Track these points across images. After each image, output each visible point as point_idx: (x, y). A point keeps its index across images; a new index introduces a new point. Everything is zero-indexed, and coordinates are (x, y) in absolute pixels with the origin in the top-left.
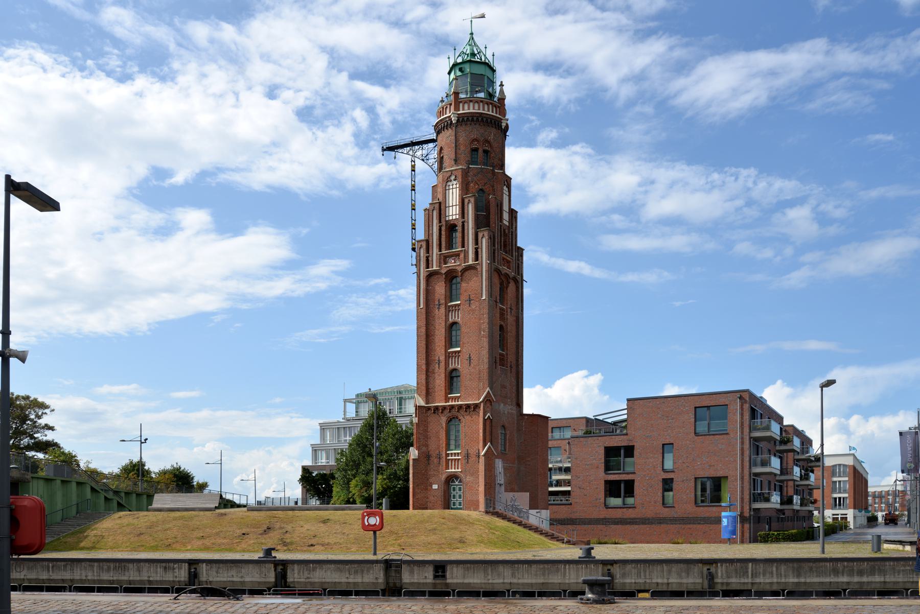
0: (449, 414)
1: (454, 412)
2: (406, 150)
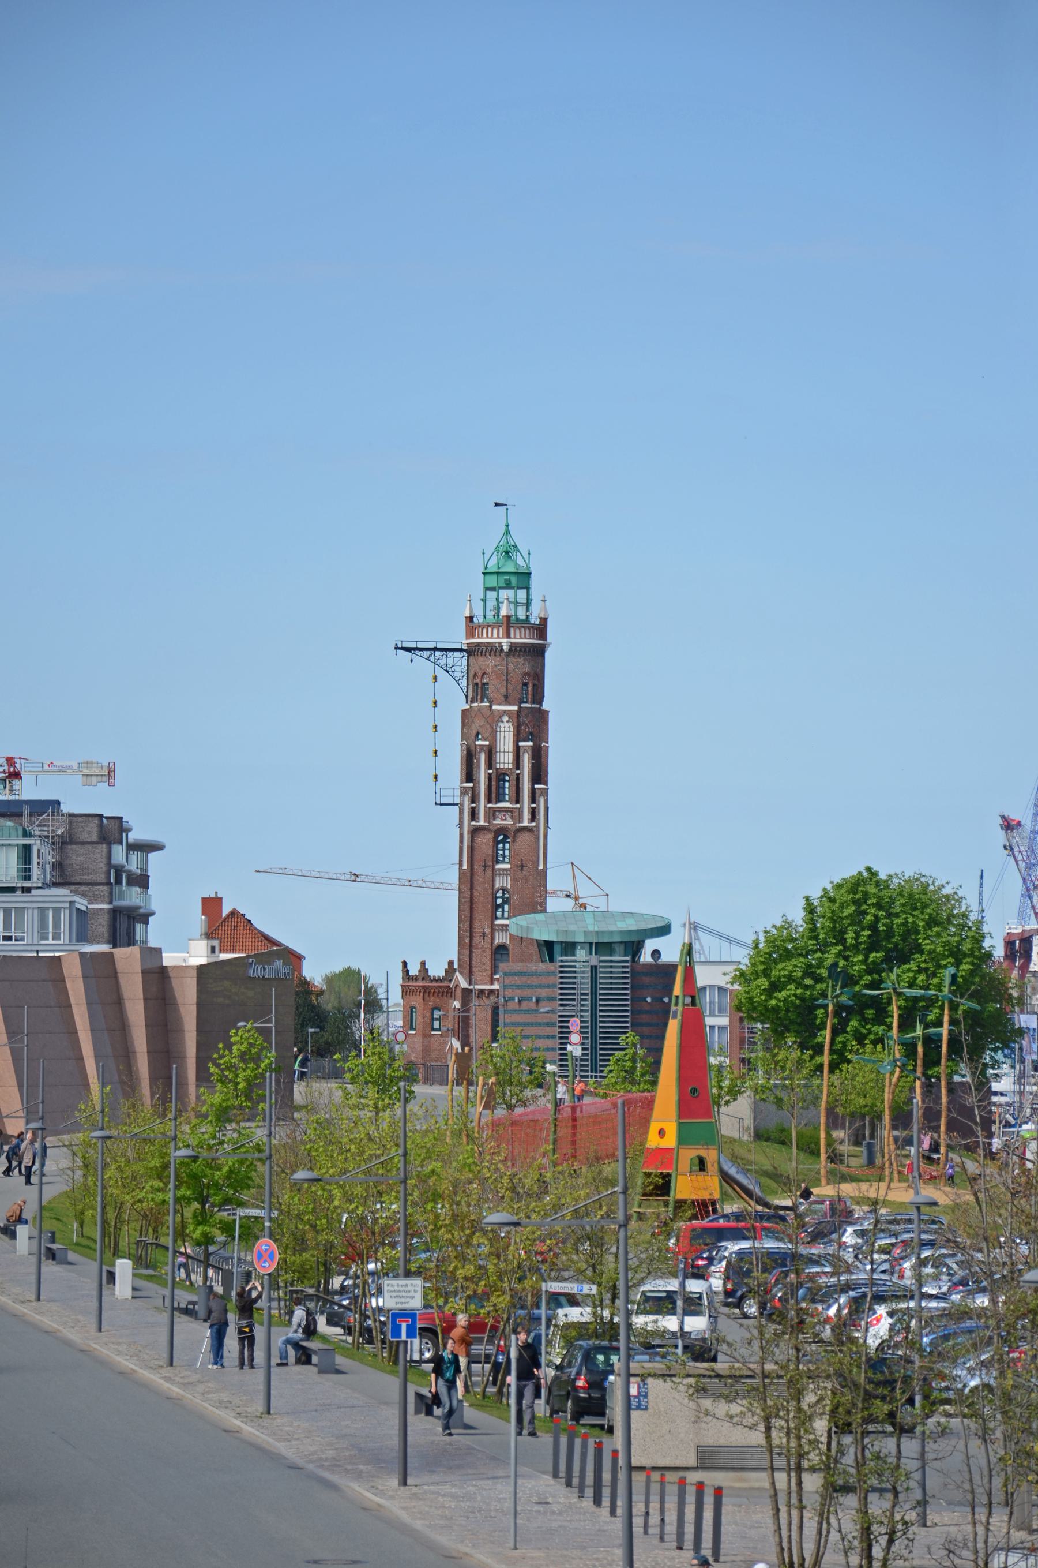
2: (426, 654)
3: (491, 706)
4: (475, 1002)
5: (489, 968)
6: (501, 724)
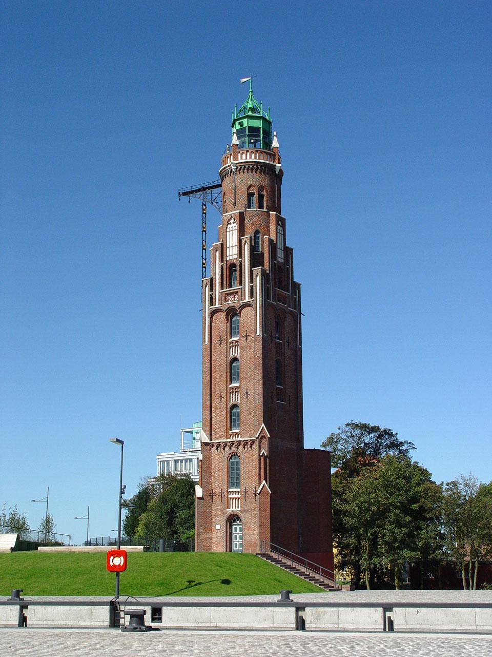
0: (230, 451)
1: (234, 448)
4: (216, 454)
5: (225, 424)
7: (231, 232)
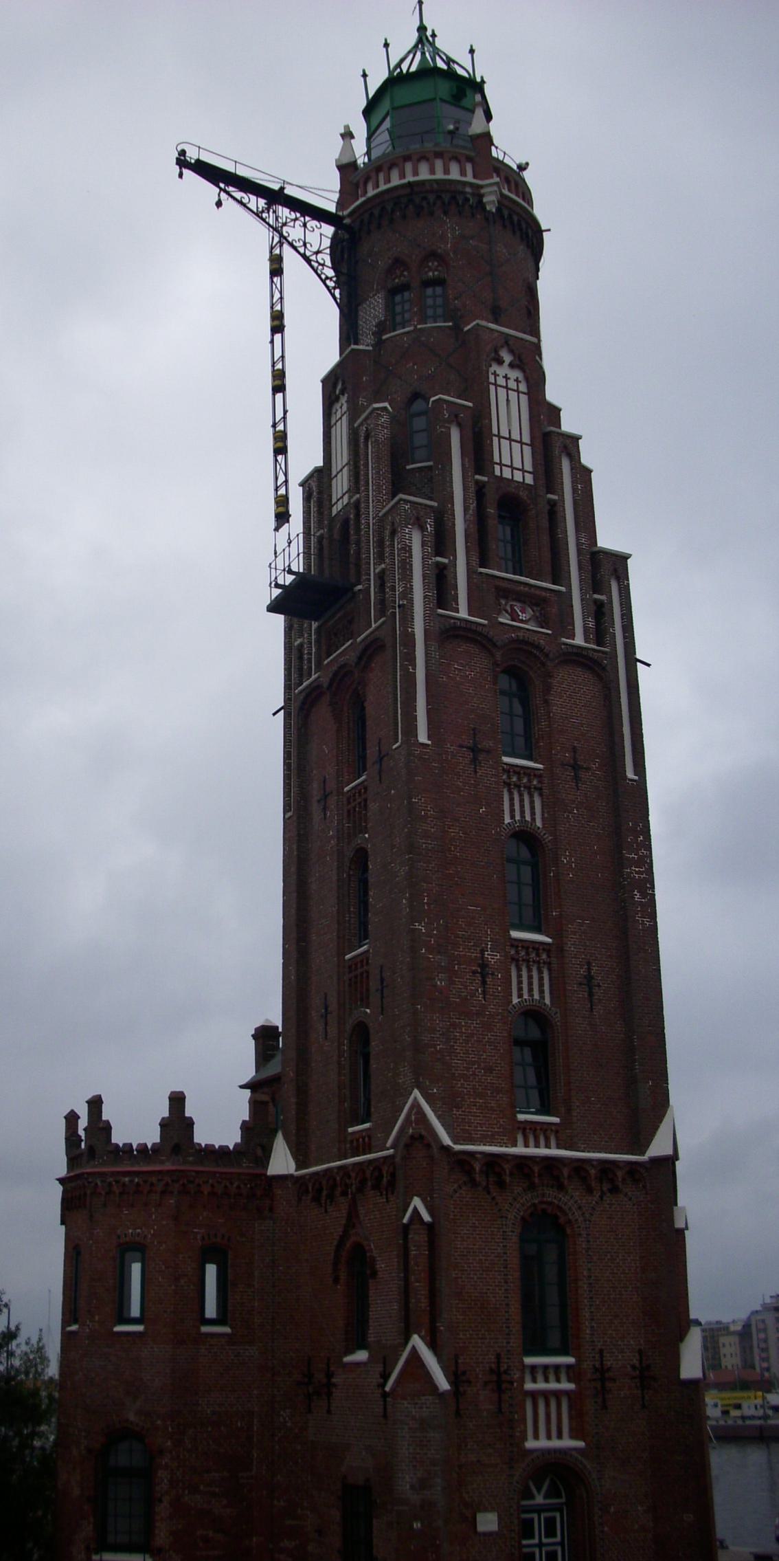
3: (457, 329)
6: (494, 367)
7: (502, 392)
